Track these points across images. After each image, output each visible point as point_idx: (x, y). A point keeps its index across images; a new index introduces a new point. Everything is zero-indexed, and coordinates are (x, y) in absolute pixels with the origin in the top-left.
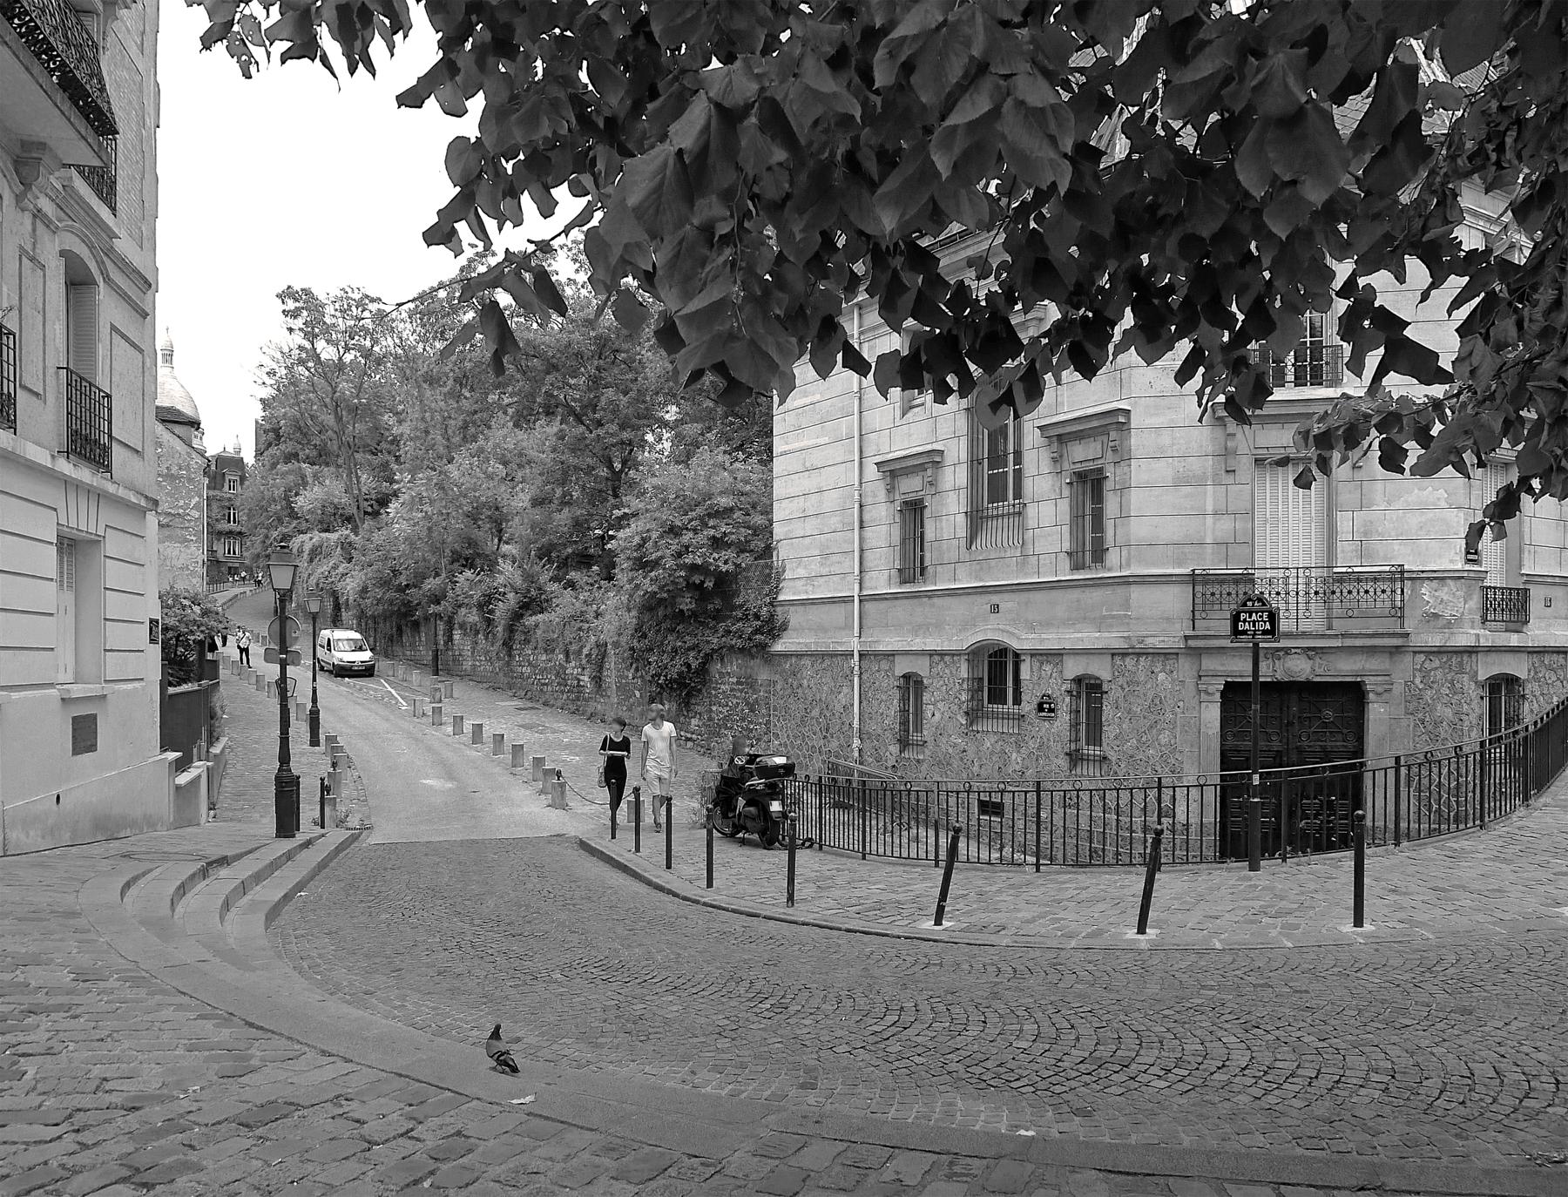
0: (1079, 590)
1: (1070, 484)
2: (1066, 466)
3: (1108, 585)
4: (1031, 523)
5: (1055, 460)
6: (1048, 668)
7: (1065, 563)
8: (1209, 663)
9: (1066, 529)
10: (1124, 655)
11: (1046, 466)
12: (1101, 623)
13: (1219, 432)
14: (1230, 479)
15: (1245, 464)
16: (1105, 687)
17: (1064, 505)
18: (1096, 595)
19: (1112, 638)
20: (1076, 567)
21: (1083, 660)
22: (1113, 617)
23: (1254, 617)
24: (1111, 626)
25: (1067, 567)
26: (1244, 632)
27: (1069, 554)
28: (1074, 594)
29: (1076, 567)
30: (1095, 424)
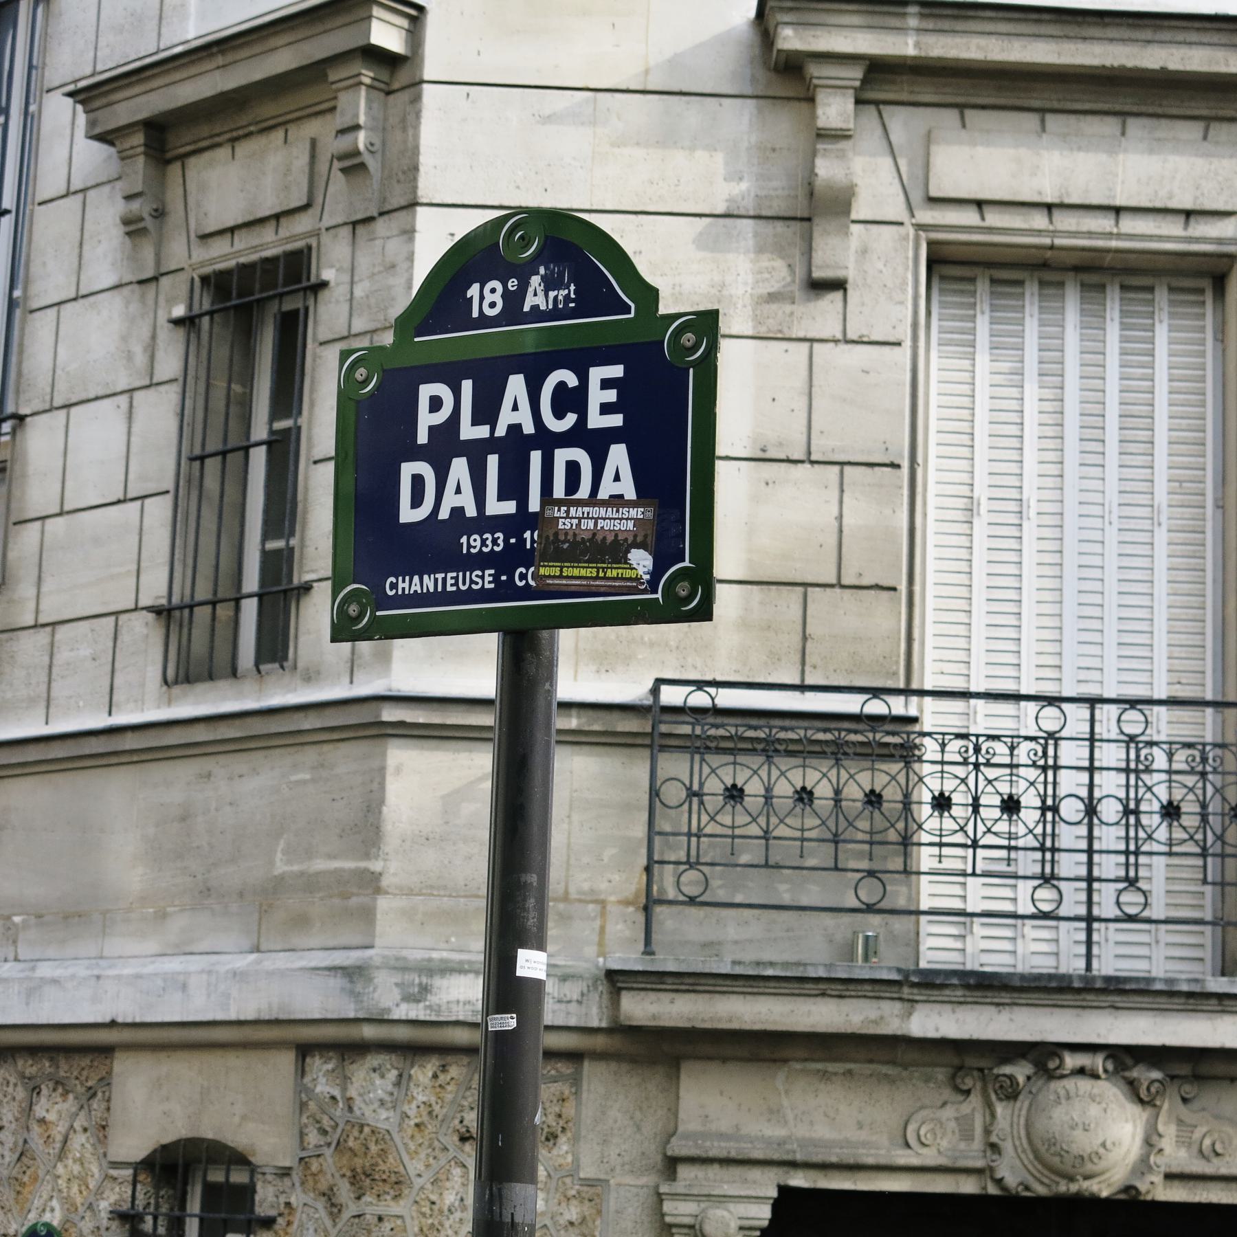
0: (184, 771)
1: (187, 323)
2: (178, 252)
3: (294, 740)
4: (38, 493)
5: (133, 228)
6: (54, 1109)
7: (144, 645)
8: (715, 1105)
9: (159, 510)
10: (349, 1050)
11: (106, 259)
12: (272, 908)
13: (784, 125)
14: (823, 315)
15: (881, 263)
16: (266, 1199)
17: (159, 415)
18: (253, 789)
19: (290, 981)
20: (186, 672)
21: (186, 1072)
22: (310, 883)
23: (516, 408)
24: (301, 922)
25: (154, 673)
26: (437, 545)
27: (163, 613)
28: (174, 784)
29: (186, 672)
30: (282, 59)
